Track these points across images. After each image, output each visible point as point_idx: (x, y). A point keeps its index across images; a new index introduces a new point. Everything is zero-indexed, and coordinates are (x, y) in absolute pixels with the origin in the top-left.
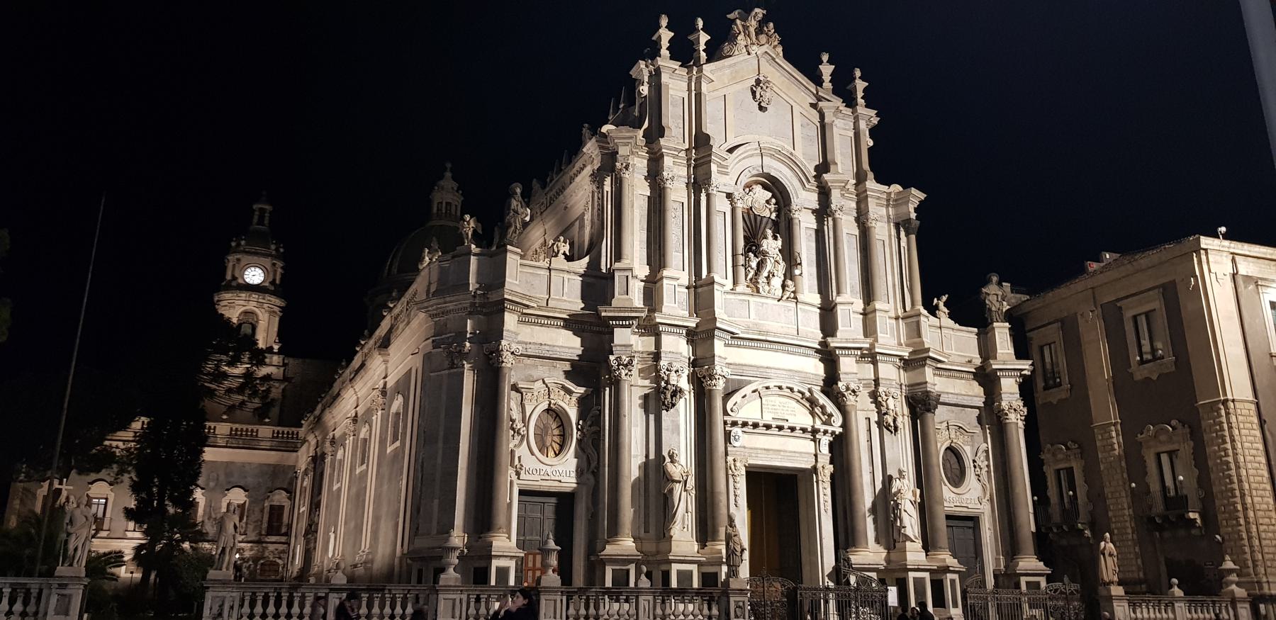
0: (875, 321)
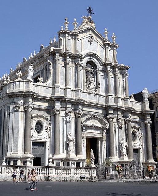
0: (117, 100)
